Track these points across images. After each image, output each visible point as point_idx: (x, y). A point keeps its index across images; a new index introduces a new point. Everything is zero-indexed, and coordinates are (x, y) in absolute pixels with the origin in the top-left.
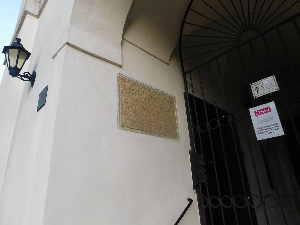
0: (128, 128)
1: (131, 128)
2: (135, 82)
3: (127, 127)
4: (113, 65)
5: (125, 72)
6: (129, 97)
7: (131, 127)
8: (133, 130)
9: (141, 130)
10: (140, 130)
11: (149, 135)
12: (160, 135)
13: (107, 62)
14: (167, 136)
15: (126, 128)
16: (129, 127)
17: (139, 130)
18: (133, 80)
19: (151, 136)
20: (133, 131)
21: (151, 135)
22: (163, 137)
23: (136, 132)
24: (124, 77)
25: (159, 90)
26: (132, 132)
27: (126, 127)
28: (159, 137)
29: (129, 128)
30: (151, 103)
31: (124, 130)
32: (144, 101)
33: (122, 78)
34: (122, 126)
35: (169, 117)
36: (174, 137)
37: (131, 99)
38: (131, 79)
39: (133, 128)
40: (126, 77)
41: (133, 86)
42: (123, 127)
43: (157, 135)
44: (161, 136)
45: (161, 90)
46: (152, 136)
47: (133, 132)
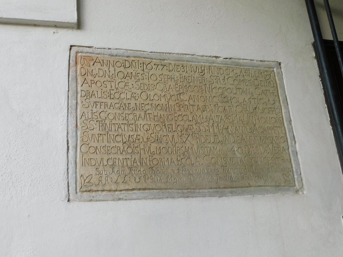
0: (104, 193)
1: (113, 189)
2: (128, 57)
3: (103, 191)
4: (52, 30)
5: (95, 37)
6: (109, 101)
7: (113, 187)
8: (122, 195)
9: (152, 189)
10: (149, 189)
11: (181, 197)
12: (225, 188)
13: (35, 25)
14: (252, 188)
15: (100, 193)
16: (107, 188)
17: (145, 189)
18: (121, 52)
19: (191, 199)
20: (120, 197)
21: (188, 197)
22: (232, 194)
23: (134, 196)
24: (90, 53)
25: (216, 57)
26: (119, 199)
27: (98, 191)
28: (220, 197)
29: (110, 191)
30: (187, 103)
31: (91, 201)
32: (163, 101)
33: (84, 58)
34: (84, 189)
35: (257, 126)
36: (276, 186)
37: (117, 106)
38: (115, 52)
39: (122, 187)
40: (99, 51)
41: (122, 69)
42: (89, 191)
43: (211, 190)
44: (227, 190)
45: (223, 55)
46: (194, 199)
47: (120, 202)
